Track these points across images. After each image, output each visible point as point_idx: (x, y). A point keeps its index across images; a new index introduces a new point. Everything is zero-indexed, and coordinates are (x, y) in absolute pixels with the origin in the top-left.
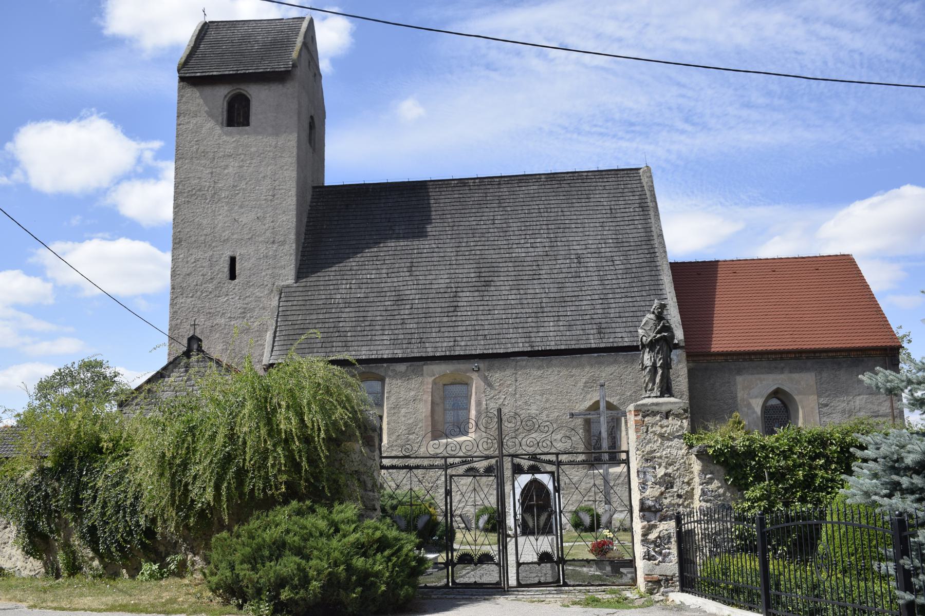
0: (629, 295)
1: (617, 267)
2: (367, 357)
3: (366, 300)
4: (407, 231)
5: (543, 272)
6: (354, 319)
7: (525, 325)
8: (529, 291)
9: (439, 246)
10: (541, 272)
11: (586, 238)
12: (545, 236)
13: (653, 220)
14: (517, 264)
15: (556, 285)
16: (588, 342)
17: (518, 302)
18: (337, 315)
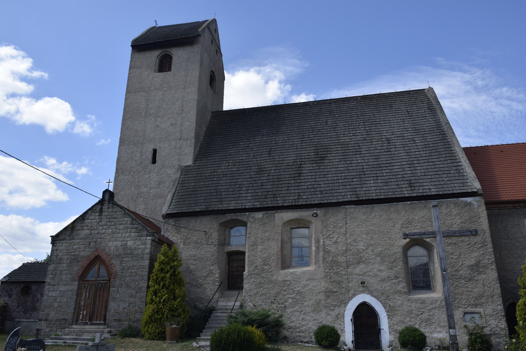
0: (430, 160)
1: (418, 144)
2: (234, 208)
3: (238, 172)
4: (268, 131)
5: (363, 150)
6: (228, 184)
7: (352, 183)
8: (353, 162)
9: (290, 138)
10: (361, 150)
11: (392, 128)
12: (363, 129)
13: (440, 115)
14: (344, 146)
15: (373, 157)
16: (402, 193)
17: (345, 168)
18: (217, 182)
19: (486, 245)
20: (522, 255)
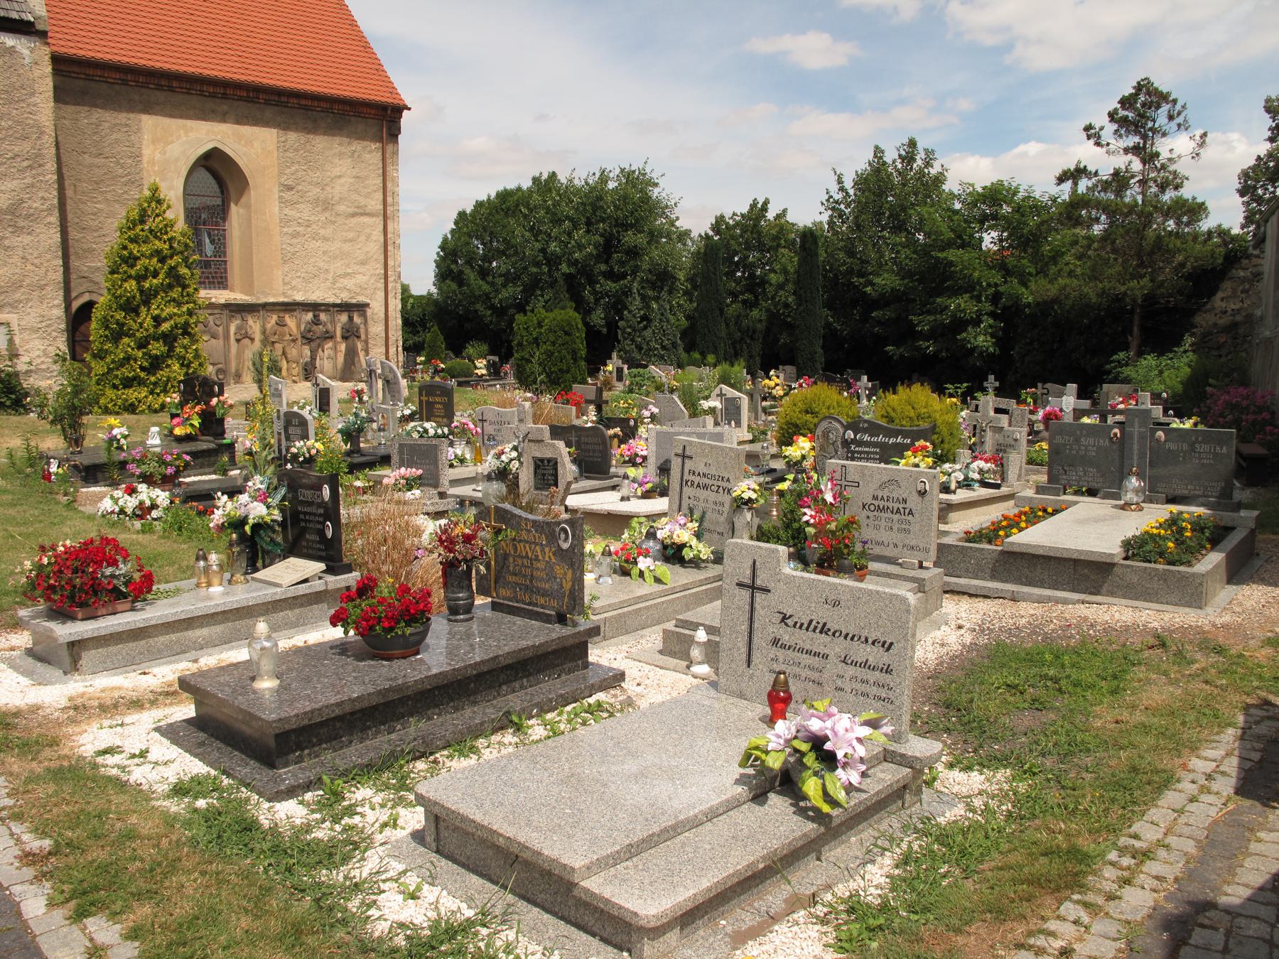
19: (40, 166)
20: (126, 196)
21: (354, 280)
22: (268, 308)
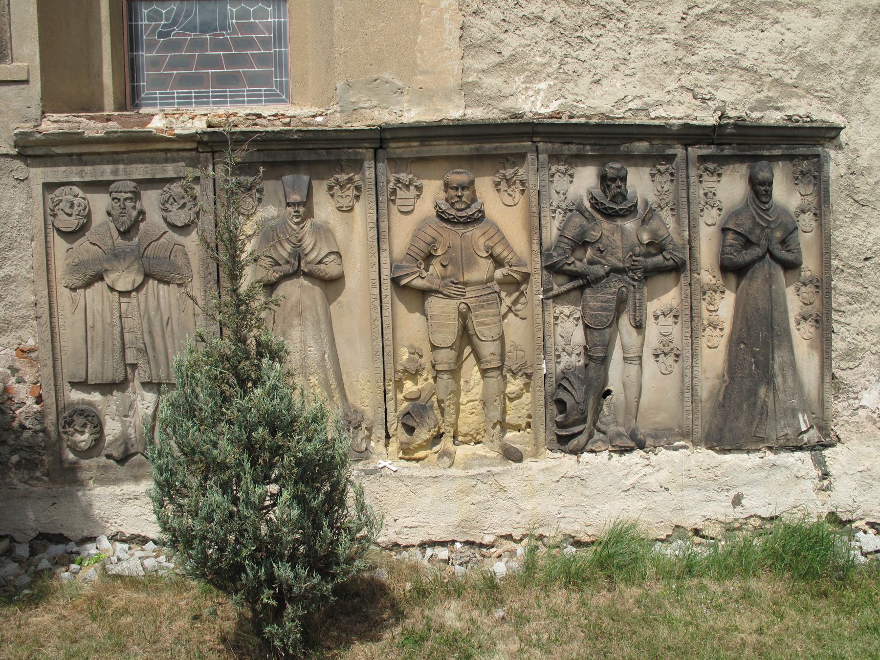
21: (773, 33)
22: (397, 149)
